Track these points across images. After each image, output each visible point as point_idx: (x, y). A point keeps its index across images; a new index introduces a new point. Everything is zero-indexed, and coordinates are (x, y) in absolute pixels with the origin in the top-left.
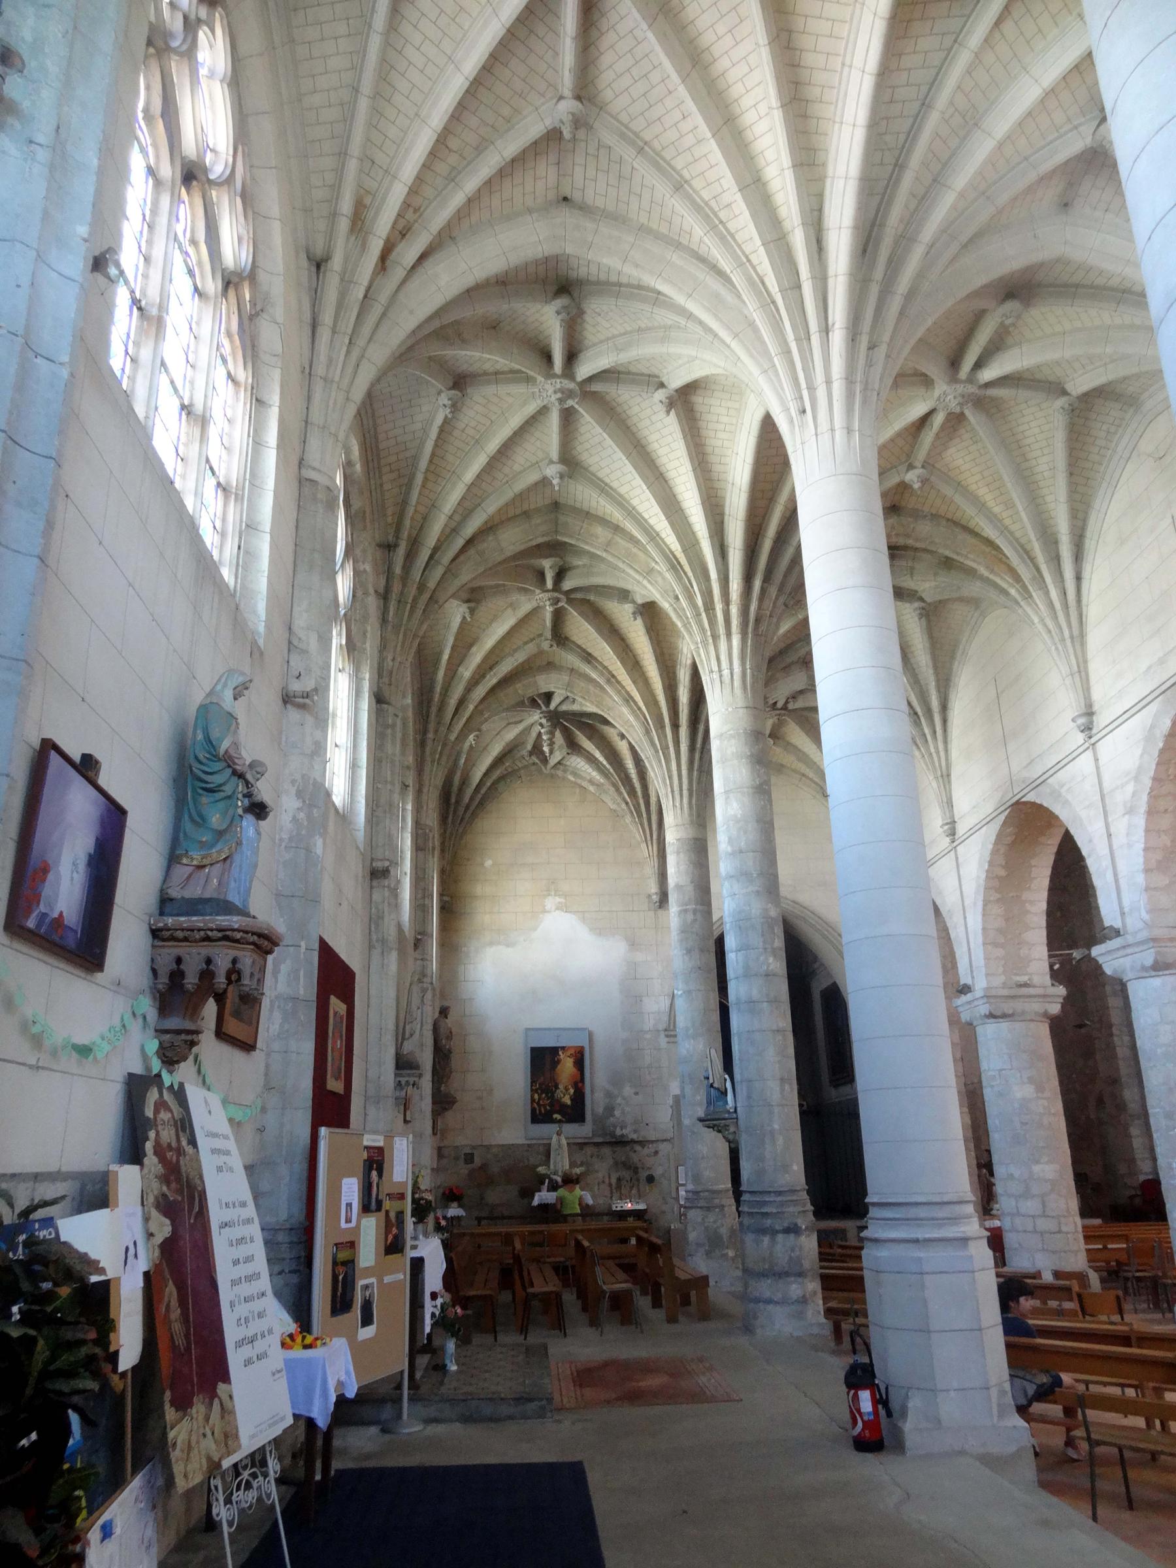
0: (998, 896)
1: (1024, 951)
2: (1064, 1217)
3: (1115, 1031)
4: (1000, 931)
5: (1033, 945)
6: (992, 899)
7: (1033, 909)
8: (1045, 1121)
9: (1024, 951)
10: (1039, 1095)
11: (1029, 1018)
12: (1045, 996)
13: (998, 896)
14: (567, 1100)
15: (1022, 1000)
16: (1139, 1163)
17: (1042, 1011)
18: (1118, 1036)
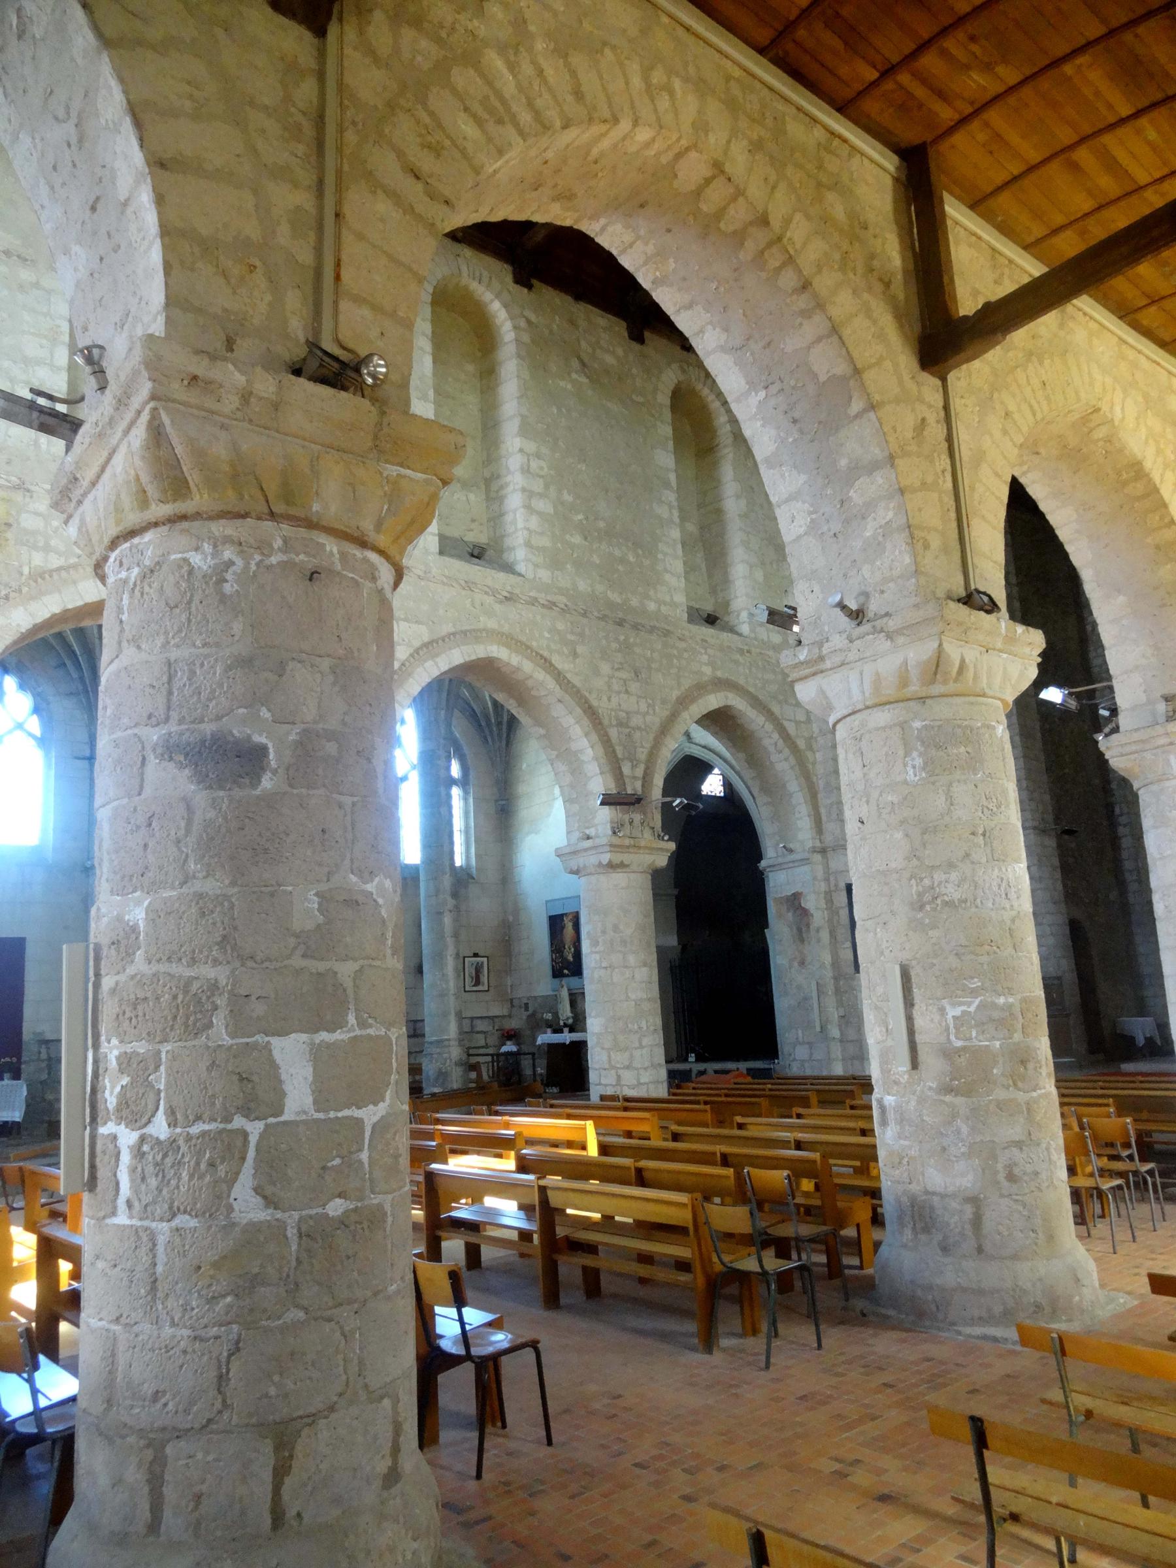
0: (555, 753)
4: (572, 786)
13: (555, 753)
14: (570, 958)
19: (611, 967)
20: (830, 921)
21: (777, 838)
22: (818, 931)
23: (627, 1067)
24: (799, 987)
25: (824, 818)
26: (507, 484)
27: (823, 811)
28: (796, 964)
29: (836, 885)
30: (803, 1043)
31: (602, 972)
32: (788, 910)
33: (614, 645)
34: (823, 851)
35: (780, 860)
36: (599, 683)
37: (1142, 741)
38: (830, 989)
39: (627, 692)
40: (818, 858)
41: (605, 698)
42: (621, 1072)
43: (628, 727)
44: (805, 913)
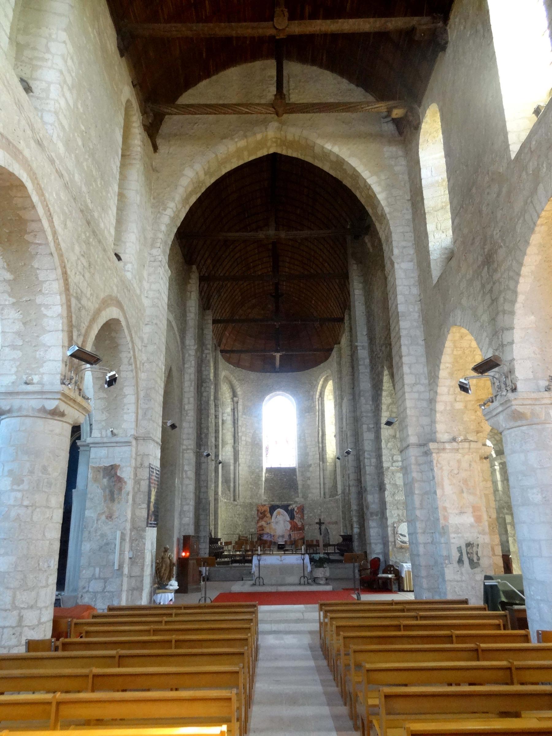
0: (12, 300)
1: (40, 353)
2: (6, 610)
3: (366, 455)
4: (19, 334)
5: (49, 347)
6: (7, 303)
7: (49, 313)
8: (13, 514)
9: (40, 353)
10: (15, 487)
11: (25, 413)
12: (42, 393)
13: (12, 300)
15: (20, 397)
16: (373, 546)
17: (40, 406)
18: (367, 458)
19: (33, 506)
20: (134, 488)
21: (104, 423)
22: (128, 494)
23: (31, 607)
24: (103, 536)
25: (140, 417)
26: (47, 60)
27: (140, 412)
28: (103, 517)
29: (141, 465)
30: (100, 578)
31: (22, 511)
32: (104, 477)
33: (84, 237)
34: (136, 439)
35: (105, 440)
36: (73, 258)
37: (536, 399)
38: (128, 539)
39: (83, 276)
40: (134, 442)
41: (73, 272)
42: (24, 612)
43: (80, 303)
44: (120, 480)
